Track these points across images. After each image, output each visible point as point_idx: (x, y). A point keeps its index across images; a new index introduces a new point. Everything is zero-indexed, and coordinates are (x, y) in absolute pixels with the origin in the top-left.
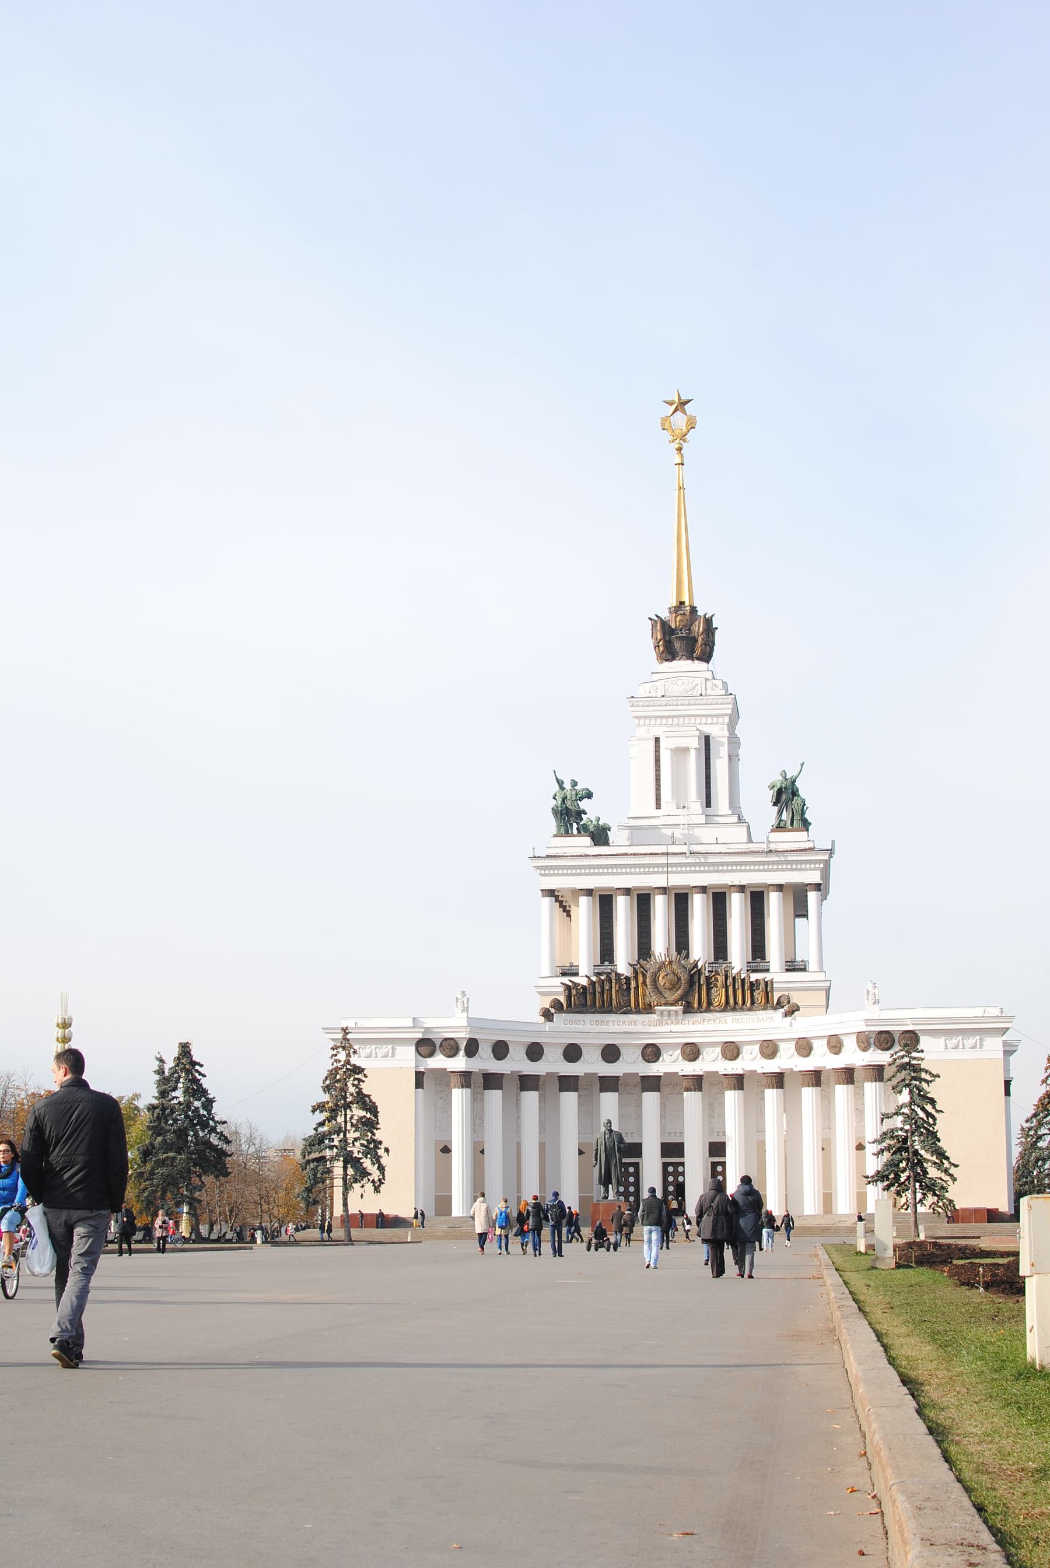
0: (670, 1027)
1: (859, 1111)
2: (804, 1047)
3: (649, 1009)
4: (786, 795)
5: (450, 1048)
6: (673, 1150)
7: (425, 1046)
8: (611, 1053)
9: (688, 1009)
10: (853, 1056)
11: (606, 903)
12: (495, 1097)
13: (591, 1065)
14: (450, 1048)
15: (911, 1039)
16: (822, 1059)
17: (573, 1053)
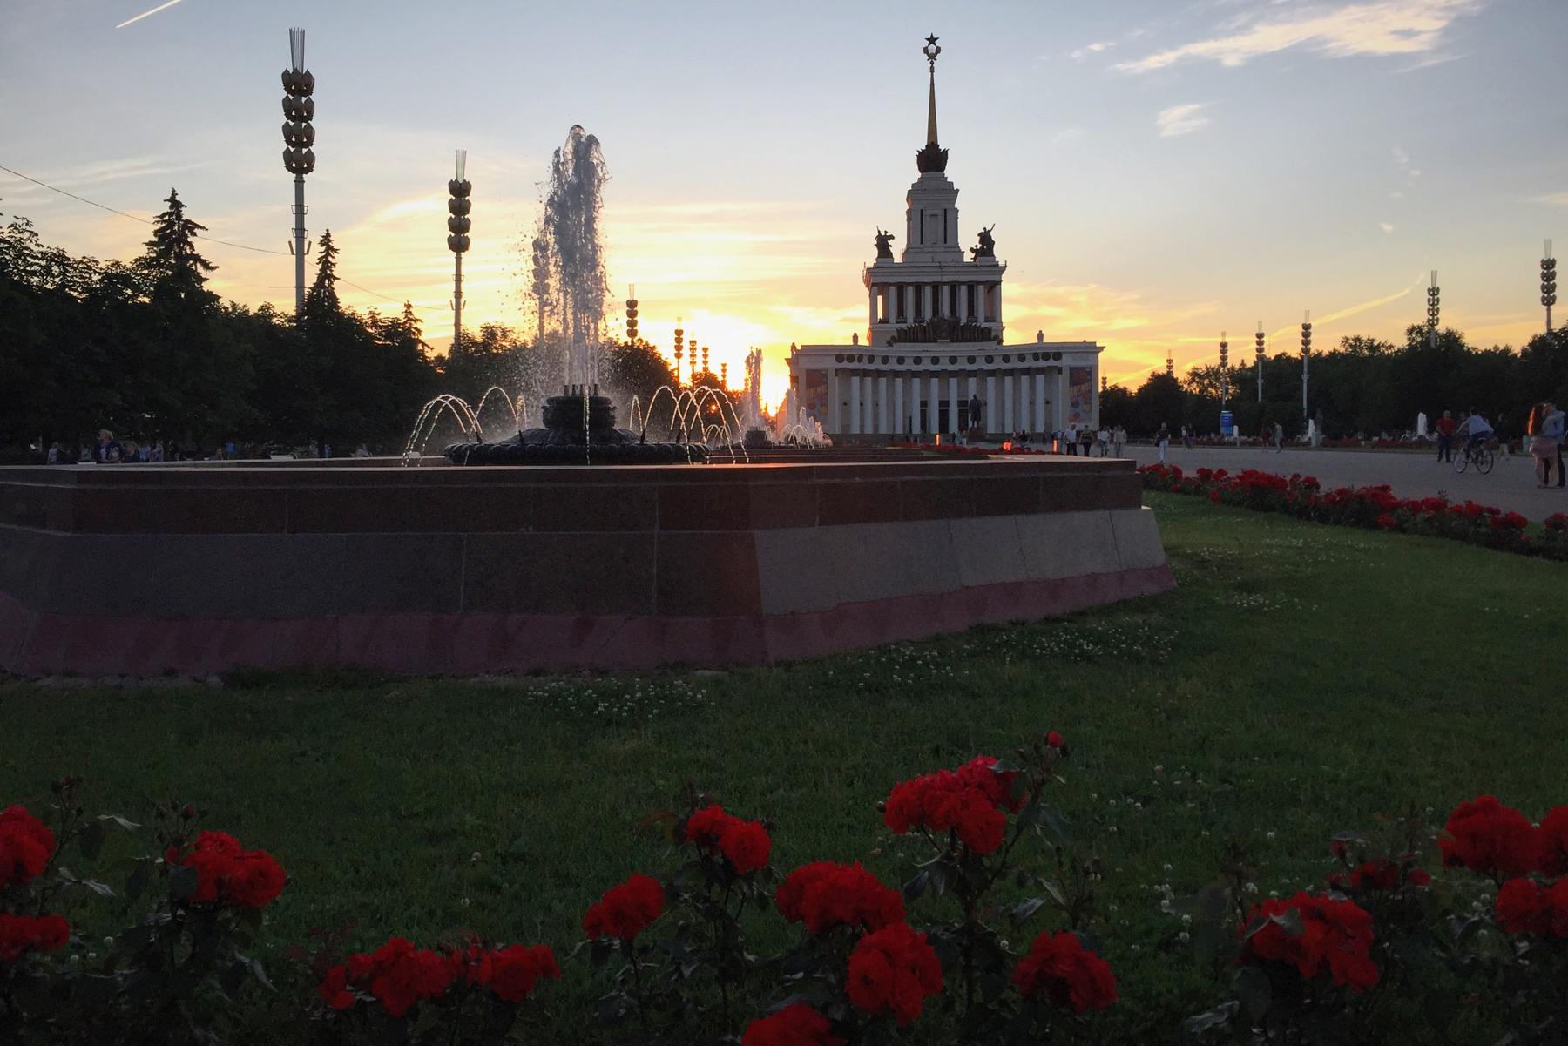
0: (944, 349)
1: (1033, 388)
2: (1006, 359)
3: (935, 341)
4: (986, 238)
5: (851, 358)
6: (944, 404)
7: (839, 358)
8: (917, 361)
9: (952, 341)
10: (1030, 363)
11: (901, 288)
12: (868, 381)
13: (909, 366)
14: (851, 358)
15: (1057, 356)
16: (1015, 364)
17: (901, 360)
